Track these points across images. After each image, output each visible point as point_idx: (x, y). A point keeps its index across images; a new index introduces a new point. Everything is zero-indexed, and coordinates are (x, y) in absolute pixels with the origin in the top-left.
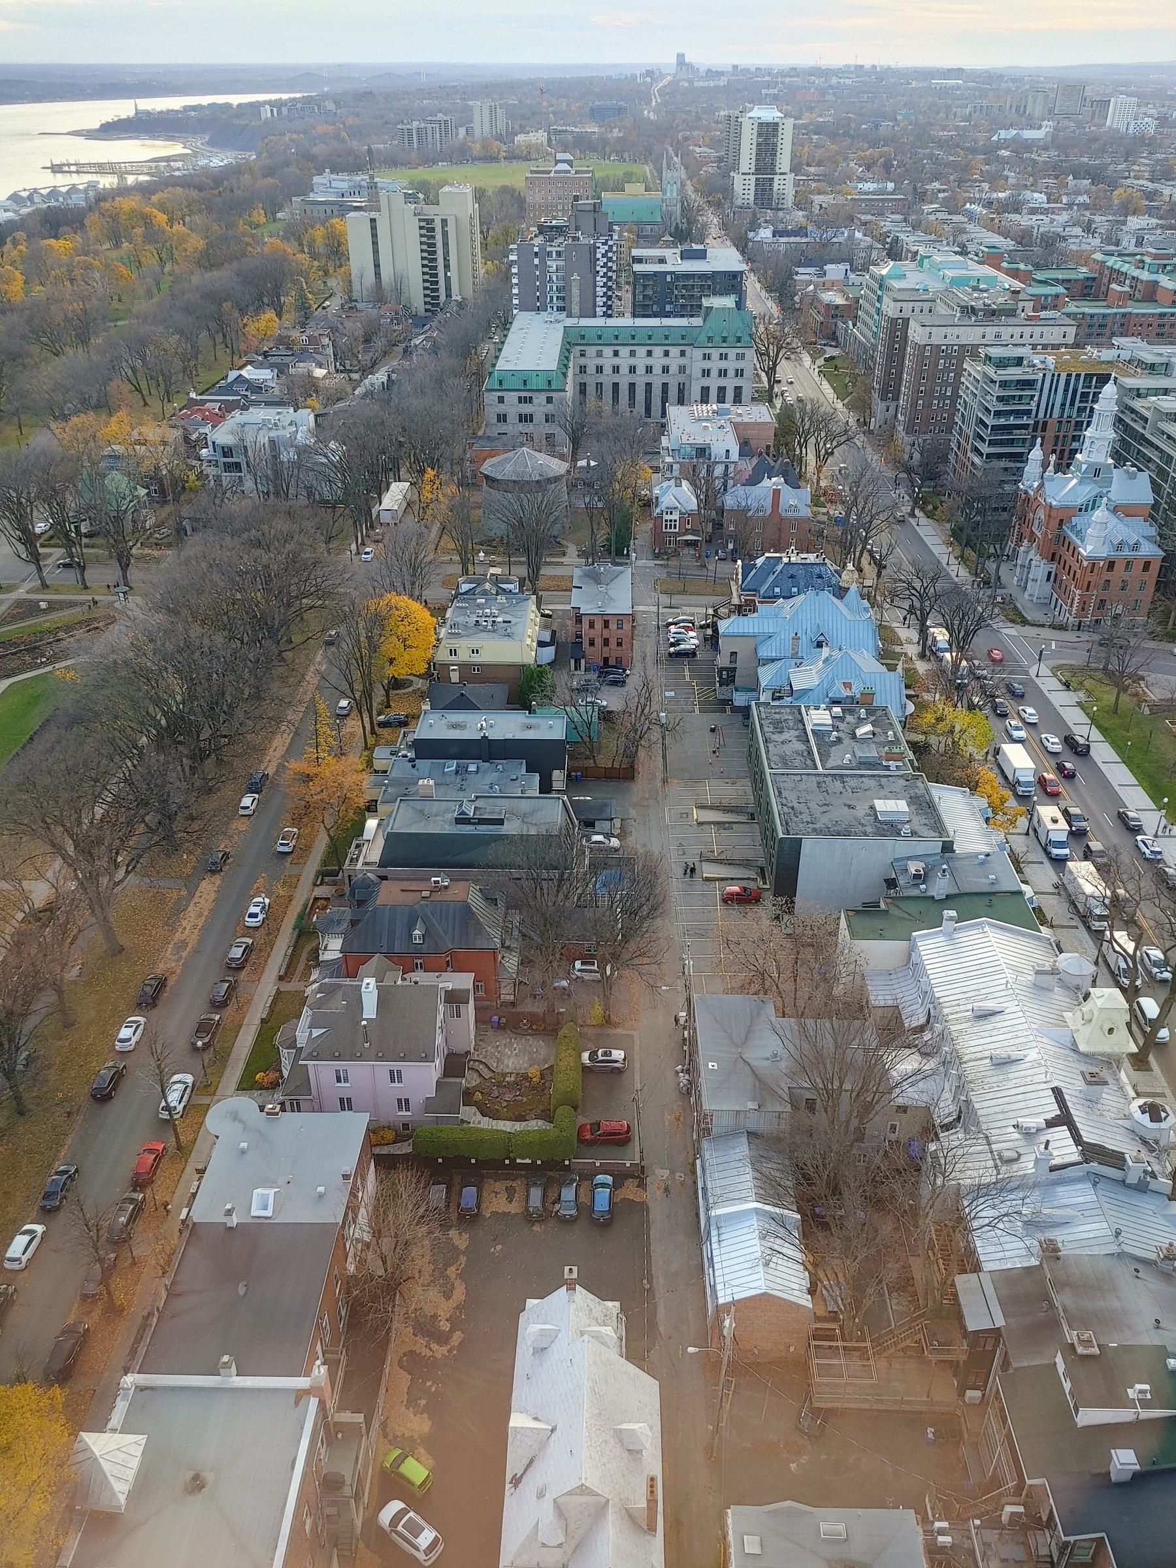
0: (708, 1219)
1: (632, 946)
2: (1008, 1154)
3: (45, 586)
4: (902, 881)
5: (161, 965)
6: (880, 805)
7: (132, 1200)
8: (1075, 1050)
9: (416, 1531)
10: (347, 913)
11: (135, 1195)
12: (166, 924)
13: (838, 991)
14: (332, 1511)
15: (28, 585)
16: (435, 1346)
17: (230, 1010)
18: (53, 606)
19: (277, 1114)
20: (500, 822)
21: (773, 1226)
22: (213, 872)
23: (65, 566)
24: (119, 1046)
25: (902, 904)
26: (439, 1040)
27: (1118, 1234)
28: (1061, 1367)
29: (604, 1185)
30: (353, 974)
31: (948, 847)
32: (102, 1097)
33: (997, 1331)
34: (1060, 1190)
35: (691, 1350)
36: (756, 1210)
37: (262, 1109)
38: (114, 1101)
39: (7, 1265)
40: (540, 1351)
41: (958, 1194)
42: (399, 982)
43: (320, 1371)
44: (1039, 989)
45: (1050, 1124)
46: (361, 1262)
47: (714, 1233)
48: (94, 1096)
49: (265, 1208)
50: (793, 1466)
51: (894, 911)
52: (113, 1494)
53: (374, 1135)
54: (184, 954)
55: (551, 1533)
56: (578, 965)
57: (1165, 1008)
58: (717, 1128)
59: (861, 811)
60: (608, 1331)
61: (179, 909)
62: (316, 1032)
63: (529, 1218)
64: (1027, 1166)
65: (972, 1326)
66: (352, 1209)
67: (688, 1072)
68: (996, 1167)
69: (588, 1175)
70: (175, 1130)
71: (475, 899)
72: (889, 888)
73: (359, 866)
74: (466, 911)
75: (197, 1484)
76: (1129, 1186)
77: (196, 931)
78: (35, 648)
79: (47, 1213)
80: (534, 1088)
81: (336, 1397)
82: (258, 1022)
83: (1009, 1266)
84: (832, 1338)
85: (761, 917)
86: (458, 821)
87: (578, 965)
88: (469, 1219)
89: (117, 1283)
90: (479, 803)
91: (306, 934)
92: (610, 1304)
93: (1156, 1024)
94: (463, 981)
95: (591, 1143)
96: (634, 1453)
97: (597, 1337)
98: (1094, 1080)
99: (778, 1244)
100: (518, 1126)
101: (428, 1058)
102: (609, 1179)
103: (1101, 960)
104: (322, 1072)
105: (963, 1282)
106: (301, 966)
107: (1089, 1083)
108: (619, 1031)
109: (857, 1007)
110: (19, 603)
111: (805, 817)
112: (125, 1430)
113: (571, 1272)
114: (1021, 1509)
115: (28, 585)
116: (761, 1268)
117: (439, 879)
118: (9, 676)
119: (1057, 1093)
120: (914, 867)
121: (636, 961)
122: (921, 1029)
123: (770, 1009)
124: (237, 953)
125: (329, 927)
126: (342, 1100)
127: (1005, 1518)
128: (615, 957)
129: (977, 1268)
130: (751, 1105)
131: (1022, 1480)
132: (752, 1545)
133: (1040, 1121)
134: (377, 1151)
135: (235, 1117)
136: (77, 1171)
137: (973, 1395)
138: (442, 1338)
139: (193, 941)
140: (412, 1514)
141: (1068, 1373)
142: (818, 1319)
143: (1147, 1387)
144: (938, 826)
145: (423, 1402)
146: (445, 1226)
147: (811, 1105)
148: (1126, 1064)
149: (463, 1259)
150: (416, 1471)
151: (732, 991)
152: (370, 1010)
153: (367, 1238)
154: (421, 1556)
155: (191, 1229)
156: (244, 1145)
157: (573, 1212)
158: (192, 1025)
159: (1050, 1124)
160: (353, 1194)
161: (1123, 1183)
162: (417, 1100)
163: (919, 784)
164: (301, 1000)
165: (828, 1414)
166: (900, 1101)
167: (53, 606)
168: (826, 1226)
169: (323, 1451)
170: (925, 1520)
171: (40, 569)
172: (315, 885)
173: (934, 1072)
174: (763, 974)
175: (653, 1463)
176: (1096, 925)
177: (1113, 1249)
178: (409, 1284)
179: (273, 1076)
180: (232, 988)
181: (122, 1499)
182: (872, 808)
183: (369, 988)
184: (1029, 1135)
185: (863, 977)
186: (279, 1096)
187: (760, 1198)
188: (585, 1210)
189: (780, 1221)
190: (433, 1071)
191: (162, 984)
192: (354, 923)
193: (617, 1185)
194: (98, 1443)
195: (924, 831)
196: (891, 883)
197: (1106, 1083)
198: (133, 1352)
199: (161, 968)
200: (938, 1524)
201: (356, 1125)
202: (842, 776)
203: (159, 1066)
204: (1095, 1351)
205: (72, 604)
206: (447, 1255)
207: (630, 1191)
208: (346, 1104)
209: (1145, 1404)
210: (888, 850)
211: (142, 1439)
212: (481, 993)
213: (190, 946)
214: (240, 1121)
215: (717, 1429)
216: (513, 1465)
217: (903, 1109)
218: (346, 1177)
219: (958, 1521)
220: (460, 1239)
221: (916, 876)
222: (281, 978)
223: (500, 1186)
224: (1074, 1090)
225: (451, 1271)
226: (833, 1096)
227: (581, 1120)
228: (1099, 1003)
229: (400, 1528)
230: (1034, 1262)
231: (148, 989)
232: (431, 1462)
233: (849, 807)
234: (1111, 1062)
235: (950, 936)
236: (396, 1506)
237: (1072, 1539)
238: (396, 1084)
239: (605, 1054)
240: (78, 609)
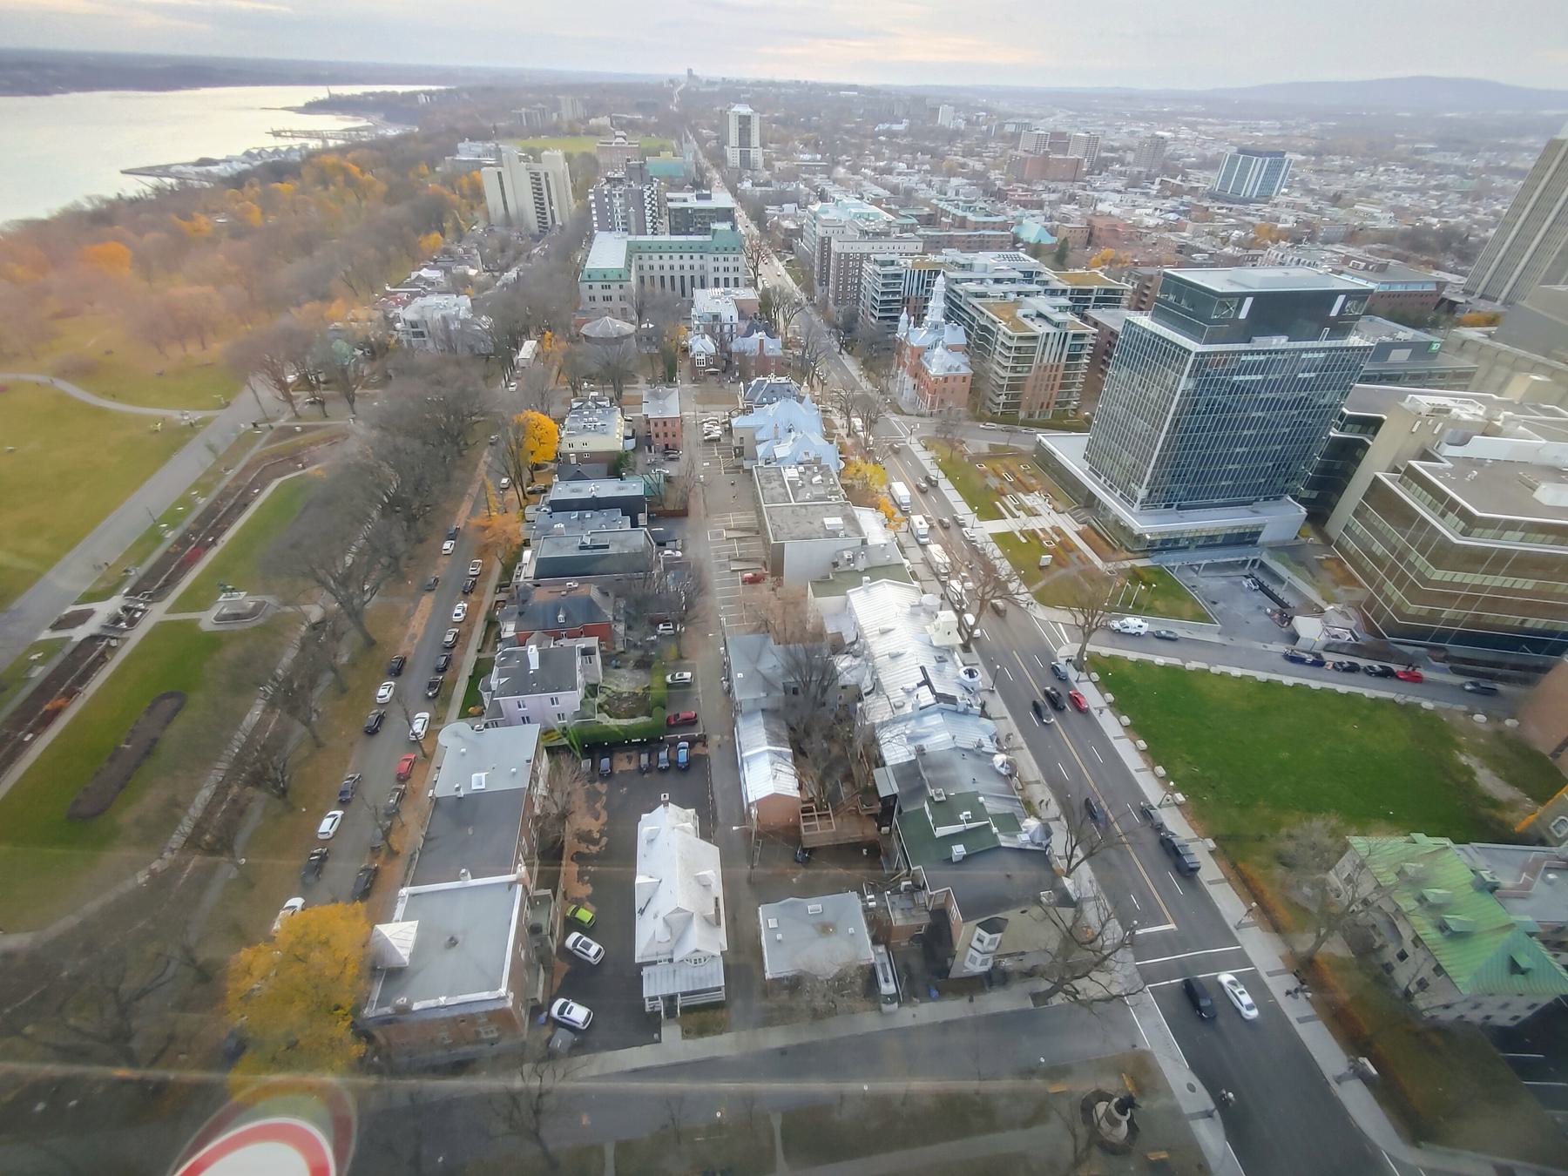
1: (690, 613)
2: (898, 704)
4: (841, 563)
6: (827, 521)
7: (398, 789)
8: (932, 646)
9: (587, 946)
11: (399, 786)
13: (809, 627)
14: (538, 944)
16: (591, 847)
17: (447, 673)
18: (305, 430)
20: (607, 547)
21: (776, 758)
22: (430, 590)
23: (311, 403)
24: (379, 700)
26: (579, 678)
27: (954, 738)
28: (927, 809)
29: (684, 748)
31: (864, 542)
32: (372, 732)
33: (895, 796)
34: (926, 719)
35: (734, 828)
36: (769, 751)
37: (473, 728)
39: (320, 837)
40: (651, 841)
41: (873, 727)
42: (552, 646)
43: (522, 869)
44: (913, 615)
45: (919, 685)
46: (543, 808)
47: (745, 765)
48: (366, 732)
50: (794, 880)
51: (838, 580)
52: (400, 957)
53: (546, 733)
54: (415, 642)
55: (662, 934)
56: (661, 626)
57: (978, 618)
58: (745, 708)
59: (817, 525)
60: (689, 825)
63: (641, 771)
65: (882, 795)
66: (534, 778)
67: (728, 680)
69: (674, 743)
70: (421, 747)
71: (594, 593)
73: (521, 579)
74: (591, 602)
75: (453, 942)
76: (960, 713)
79: (343, 804)
80: (639, 699)
81: (534, 881)
82: (467, 678)
84: (812, 811)
85: (764, 589)
86: (581, 548)
87: (661, 626)
88: (607, 777)
89: (393, 838)
90: (593, 536)
91: (492, 624)
92: (689, 811)
93: (973, 628)
94: (593, 642)
95: (673, 726)
96: (707, 887)
97: (683, 829)
98: (941, 660)
99: (778, 766)
100: (632, 721)
101: (574, 688)
102: (687, 744)
104: (508, 703)
105: (877, 772)
106: (491, 643)
107: (939, 662)
108: (687, 662)
109: (819, 634)
110: (282, 428)
111: (786, 531)
112: (405, 919)
113: (665, 796)
114: (910, 883)
116: (771, 780)
117: (572, 584)
119: (923, 669)
120: (847, 555)
121: (696, 620)
122: (853, 643)
124: (449, 638)
125: (507, 617)
126: (523, 718)
128: (682, 620)
129: (884, 765)
130: (763, 695)
131: (910, 869)
132: (773, 923)
135: (457, 735)
137: (885, 829)
138: (595, 842)
140: (585, 938)
142: (804, 802)
143: (969, 813)
144: (859, 531)
145: (587, 878)
146: (592, 781)
147: (795, 691)
148: (959, 649)
149: (604, 798)
150: (585, 915)
151: (748, 634)
152: (534, 664)
153: (545, 793)
154: (592, 960)
155: (436, 802)
156: (463, 750)
157: (668, 765)
158: (425, 683)
159: (919, 685)
160: (534, 770)
161: (956, 711)
162: (569, 713)
164: (492, 662)
165: (812, 851)
166: (841, 683)
168: (803, 754)
169: (529, 913)
170: (862, 896)
171: (293, 406)
172: (496, 593)
174: (766, 622)
175: (718, 890)
176: (944, 578)
177: (953, 746)
178: (573, 816)
181: (406, 959)
182: (823, 523)
183: (533, 652)
184: (909, 692)
185: (822, 618)
186: (484, 720)
187: (769, 744)
188: (674, 763)
189: (779, 754)
190: (579, 694)
191: (403, 661)
192: (521, 614)
193: (692, 745)
194: (385, 930)
195: (851, 534)
196: (835, 565)
197: (946, 661)
198: (406, 875)
199: (401, 653)
200: (869, 897)
201: (533, 731)
205: (318, 428)
206: (593, 796)
207: (699, 749)
209: (968, 821)
211: (416, 923)
212: (603, 648)
216: (638, 905)
217: (844, 687)
218: (529, 761)
219: (878, 893)
220: (602, 788)
221: (849, 560)
222: (479, 651)
223: (623, 756)
224: (931, 666)
225: (598, 806)
226: (807, 685)
227: (668, 714)
228: (943, 619)
229: (578, 947)
230: (913, 757)
232: (594, 909)
234: (950, 650)
236: (575, 935)
237: (934, 893)
238: (556, 705)
239: (680, 675)
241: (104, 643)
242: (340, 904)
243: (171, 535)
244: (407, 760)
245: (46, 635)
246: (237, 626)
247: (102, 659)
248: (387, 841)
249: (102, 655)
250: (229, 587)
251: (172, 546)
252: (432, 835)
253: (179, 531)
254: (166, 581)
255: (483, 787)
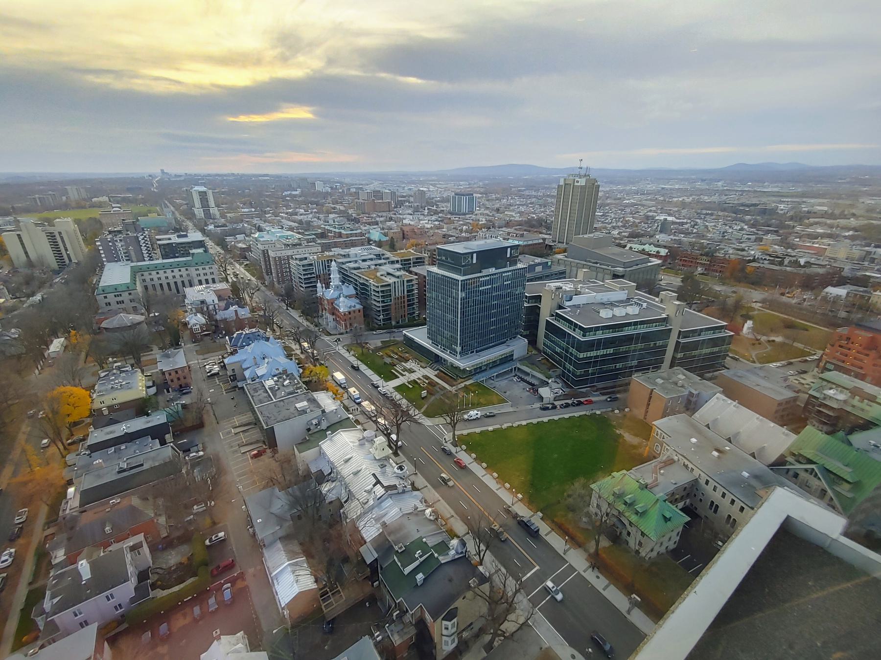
0: (271, 578)
2: (364, 502)
4: (312, 428)
6: (298, 405)
8: (376, 460)
10: (63, 536)
13: (300, 472)
19: (37, 652)
20: (142, 465)
25: (313, 435)
26: (130, 569)
27: (401, 509)
30: (75, 562)
31: (323, 411)
34: (383, 504)
37: (26, 655)
44: (362, 445)
45: (374, 485)
47: (275, 582)
57: (398, 435)
59: (292, 410)
60: (240, 645)
62: (55, 600)
63: (196, 621)
64: (371, 502)
68: (363, 507)
71: (135, 501)
72: (308, 432)
73: (68, 512)
74: (133, 509)
83: (374, 536)
84: (328, 593)
85: (266, 459)
86: (119, 472)
90: (128, 461)
92: (238, 634)
93: (397, 441)
94: (140, 537)
97: (237, 651)
98: (383, 466)
100: (182, 586)
102: (229, 585)
103: (378, 429)
104: (64, 618)
108: (220, 525)
111: (273, 418)
119: (374, 475)
122: (330, 473)
123: (277, 490)
125: (56, 547)
127: (394, 618)
128: (211, 498)
129: (365, 542)
130: (278, 528)
133: (371, 486)
134: (109, 636)
141: (399, 561)
142: (321, 589)
143: (420, 551)
144: (319, 406)
147: (299, 517)
148: (393, 456)
159: (374, 485)
163: (309, 394)
170: (371, 635)
173: (334, 487)
174: (272, 480)
176: (374, 419)
177: (401, 514)
179: (33, 635)
182: (296, 407)
184: (369, 492)
186: (40, 643)
188: (221, 603)
190: (133, 582)
192: (69, 539)
195: (313, 409)
196: (309, 430)
197: (386, 466)
202: (282, 400)
204: (404, 548)
207: (240, 584)
208: (84, 624)
209: (421, 557)
210: (304, 418)
212: (150, 539)
215: (294, 653)
217: (331, 502)
219: (380, 628)
221: (316, 425)
222: (30, 584)
224: (378, 471)
228: (378, 443)
230: (381, 530)
233: (288, 409)
234: (387, 458)
235: (331, 439)
237: (413, 612)
238: (112, 600)
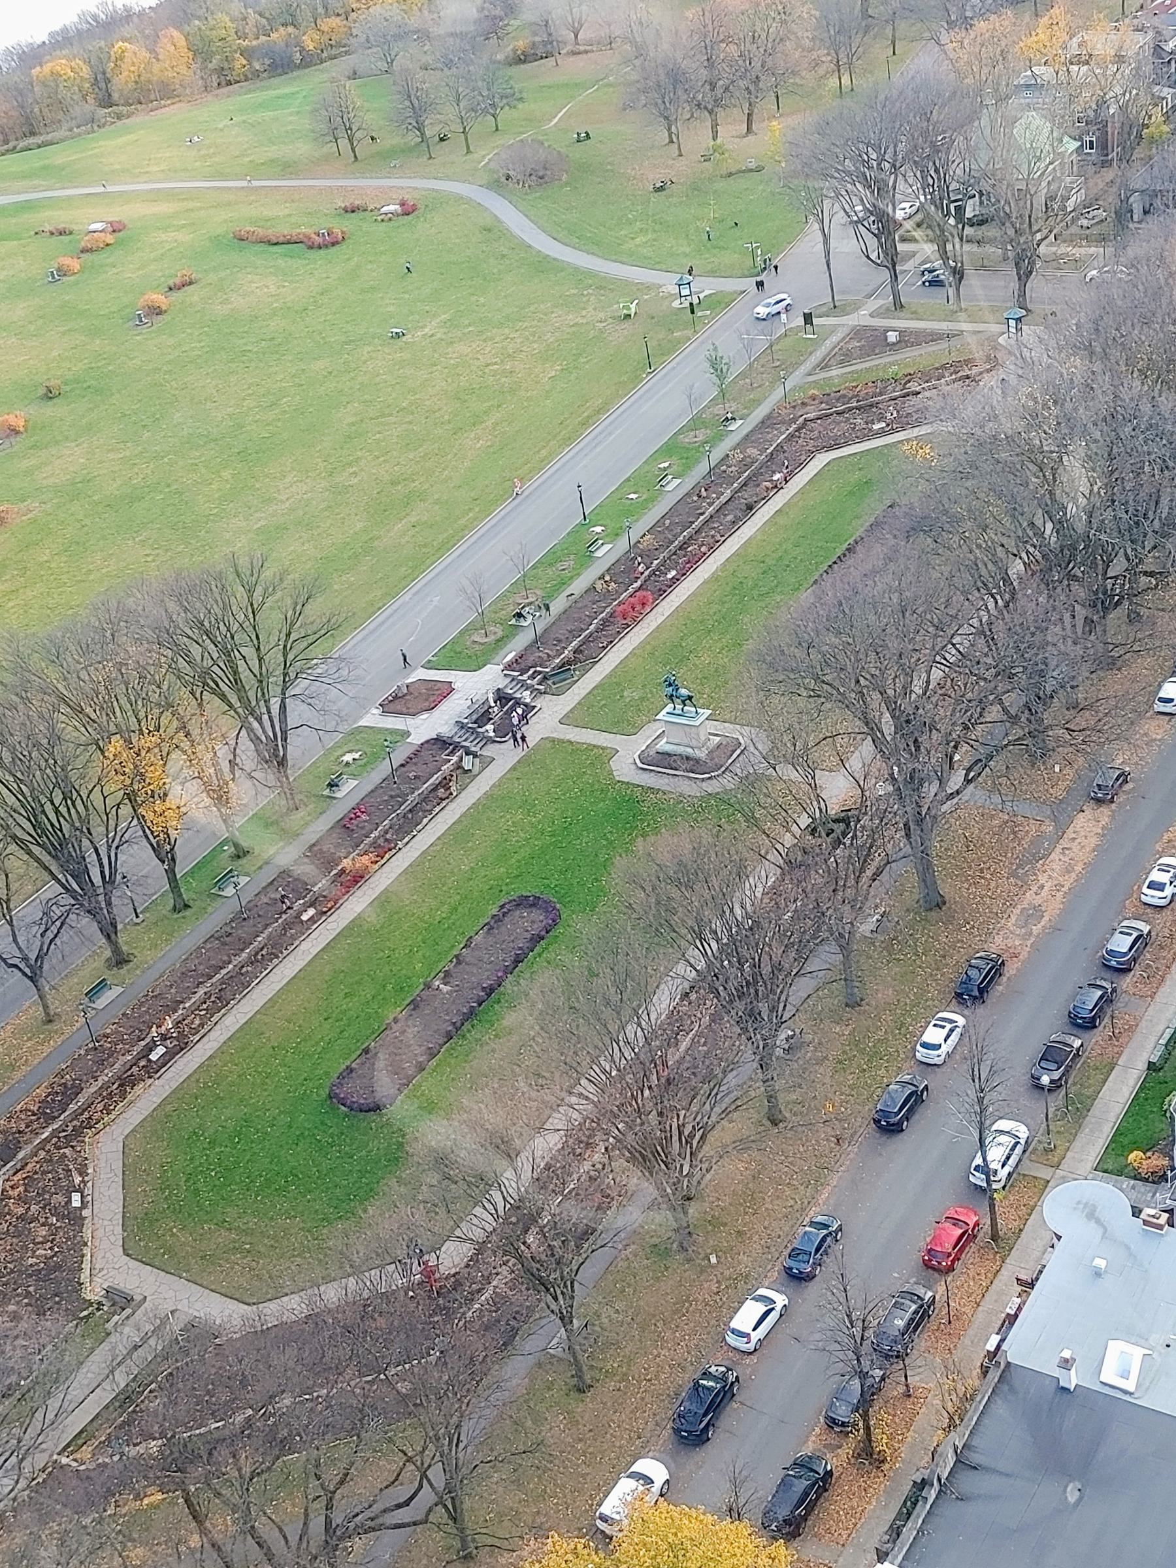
3: (898, 305)
5: (999, 940)
11: (920, 1291)
12: (1014, 874)
15: (874, 304)
19: (1160, 1227)
22: (1099, 801)
24: (921, 1054)
37: (1136, 1212)
38: (901, 1135)
39: (731, 1339)
49: (1125, 1375)
54: (1036, 930)
61: (1037, 856)
70: (992, 1206)
77: (1059, 895)
78: (872, 406)
82: (1142, 1065)
89: (879, 1414)
110: (858, 332)
115: (874, 304)
118: (830, 448)
124: (1121, 943)
135: (1091, 1214)
136: (840, 1229)
139: (1053, 909)
156: (1100, 1263)
158: (1035, 1047)
167: (907, 340)
180: (1107, 1000)
191: (996, 969)
198: (895, 1532)
199: (997, 945)
203: (980, 1101)
205: (935, 337)
213: (1046, 918)
214: (1098, 1221)
231: (973, 973)
240: (944, 345)
241: (455, 759)
242: (744, 1528)
243: (607, 553)
244: (956, 1222)
245: (373, 718)
246: (686, 787)
247: (442, 792)
248: (865, 1417)
249: (445, 783)
250: (683, 692)
251: (602, 577)
252: (975, 1458)
253: (623, 545)
254: (576, 651)
255: (1130, 1386)
